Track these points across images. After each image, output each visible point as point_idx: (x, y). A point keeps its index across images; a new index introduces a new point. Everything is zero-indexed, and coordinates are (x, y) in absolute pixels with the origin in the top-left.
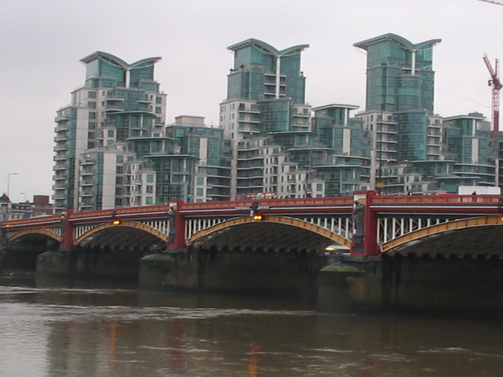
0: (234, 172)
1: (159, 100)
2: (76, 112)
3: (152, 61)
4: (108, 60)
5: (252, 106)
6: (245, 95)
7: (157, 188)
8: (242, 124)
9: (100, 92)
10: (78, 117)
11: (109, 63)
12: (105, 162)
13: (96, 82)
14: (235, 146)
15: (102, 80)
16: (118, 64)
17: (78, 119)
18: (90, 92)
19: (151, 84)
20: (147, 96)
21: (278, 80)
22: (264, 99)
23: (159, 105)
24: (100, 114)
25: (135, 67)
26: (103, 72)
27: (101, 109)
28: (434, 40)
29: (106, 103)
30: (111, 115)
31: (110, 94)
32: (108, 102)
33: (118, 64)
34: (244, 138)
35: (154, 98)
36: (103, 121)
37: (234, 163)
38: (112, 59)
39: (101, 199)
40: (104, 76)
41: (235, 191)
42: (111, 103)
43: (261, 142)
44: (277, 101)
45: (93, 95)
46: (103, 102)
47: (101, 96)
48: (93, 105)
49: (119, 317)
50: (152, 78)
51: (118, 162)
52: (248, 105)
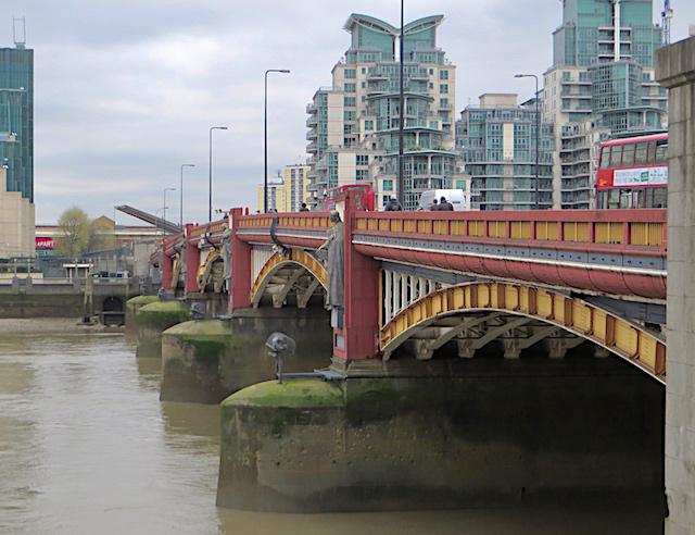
0: (557, 170)
1: (444, 75)
3: (432, 22)
5: (580, 74)
6: (570, 61)
8: (566, 102)
11: (371, 28)
13: (352, 54)
14: (558, 131)
15: (361, 52)
21: (617, 34)
22: (599, 64)
23: (444, 82)
24: (359, 100)
26: (363, 41)
27: (361, 92)
29: (367, 85)
30: (372, 99)
32: (370, 82)
34: (570, 120)
35: (436, 71)
36: (365, 109)
37: (556, 155)
38: (373, 23)
40: (364, 48)
41: (560, 195)
43: (588, 125)
44: (617, 64)
45: (351, 74)
46: (363, 84)
47: (361, 77)
48: (350, 88)
49: (306, 391)
52: (575, 75)
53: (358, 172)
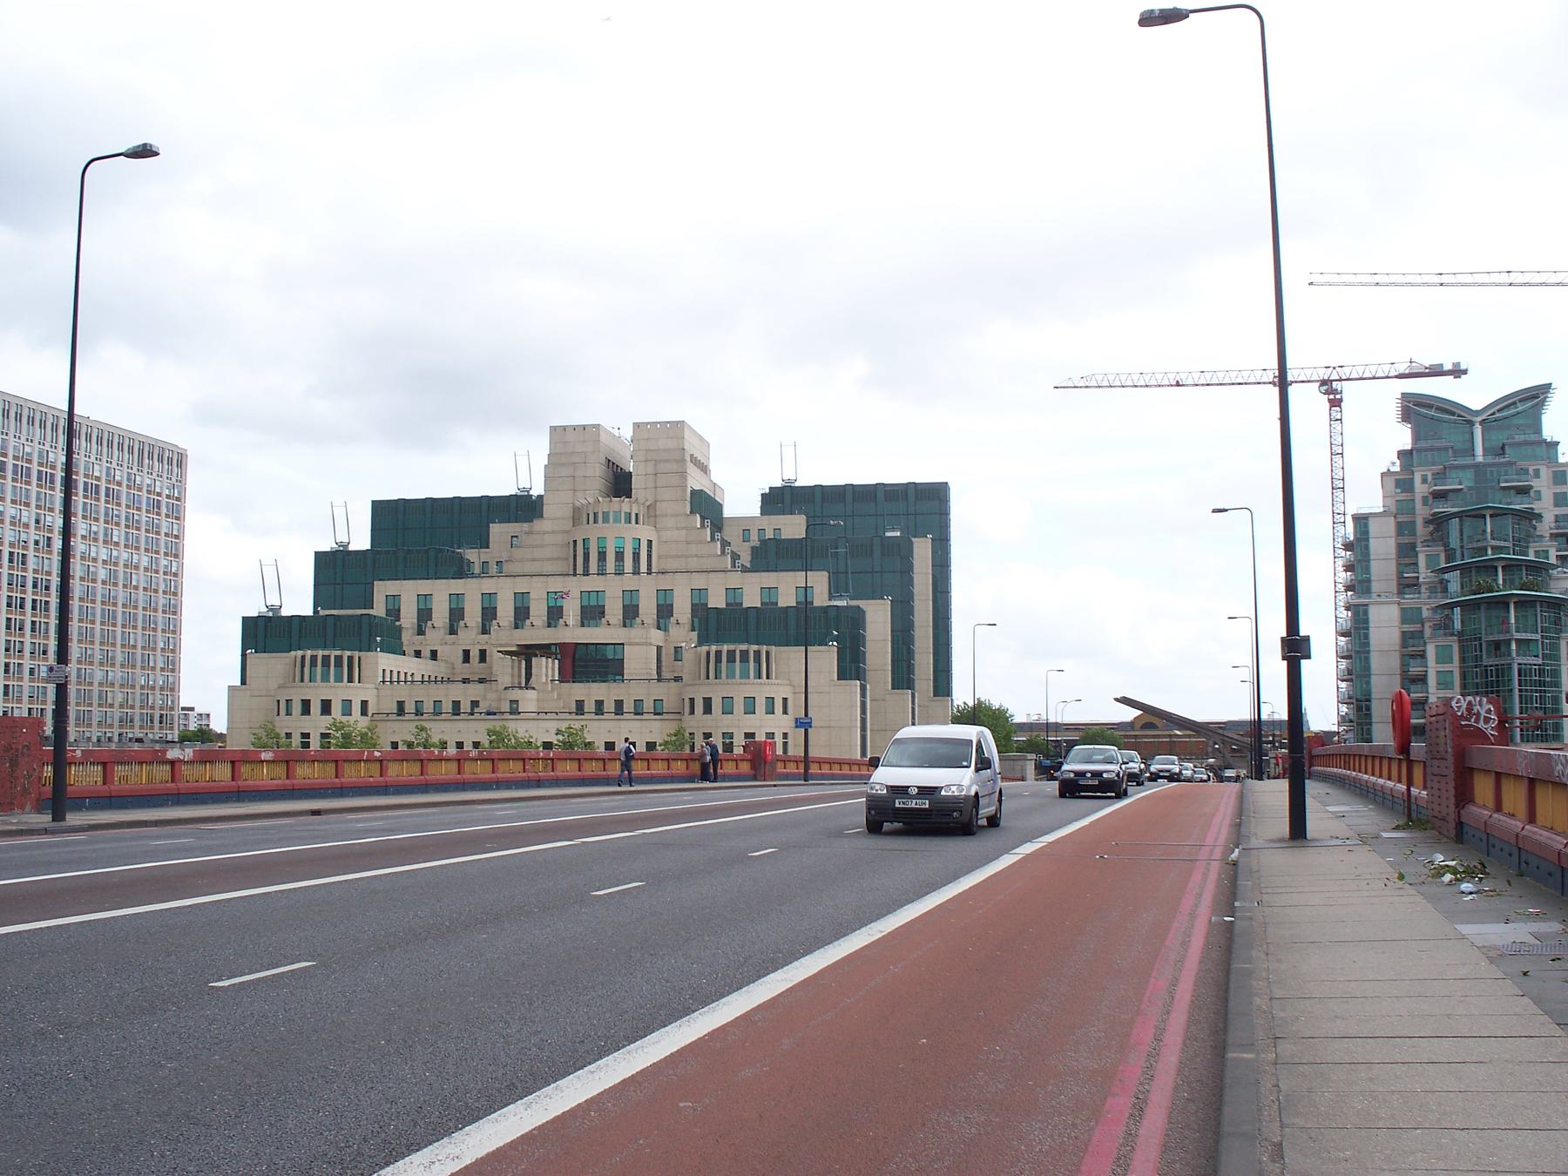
2: (1366, 525)
4: (1430, 407)
7: (1464, 676)
9: (1418, 478)
10: (1371, 535)
12: (1371, 625)
16: (1453, 414)
17: (1371, 540)
18: (1396, 480)
19: (1533, 443)
20: (1526, 472)
25: (1494, 414)
27: (1422, 512)
28: (1175, 9)
30: (1438, 523)
31: (1440, 476)
33: (1453, 414)
39: (1368, 708)
42: (1440, 496)
47: (1420, 489)
50: (1538, 430)
51: (1404, 621)
53: (1403, 633)
